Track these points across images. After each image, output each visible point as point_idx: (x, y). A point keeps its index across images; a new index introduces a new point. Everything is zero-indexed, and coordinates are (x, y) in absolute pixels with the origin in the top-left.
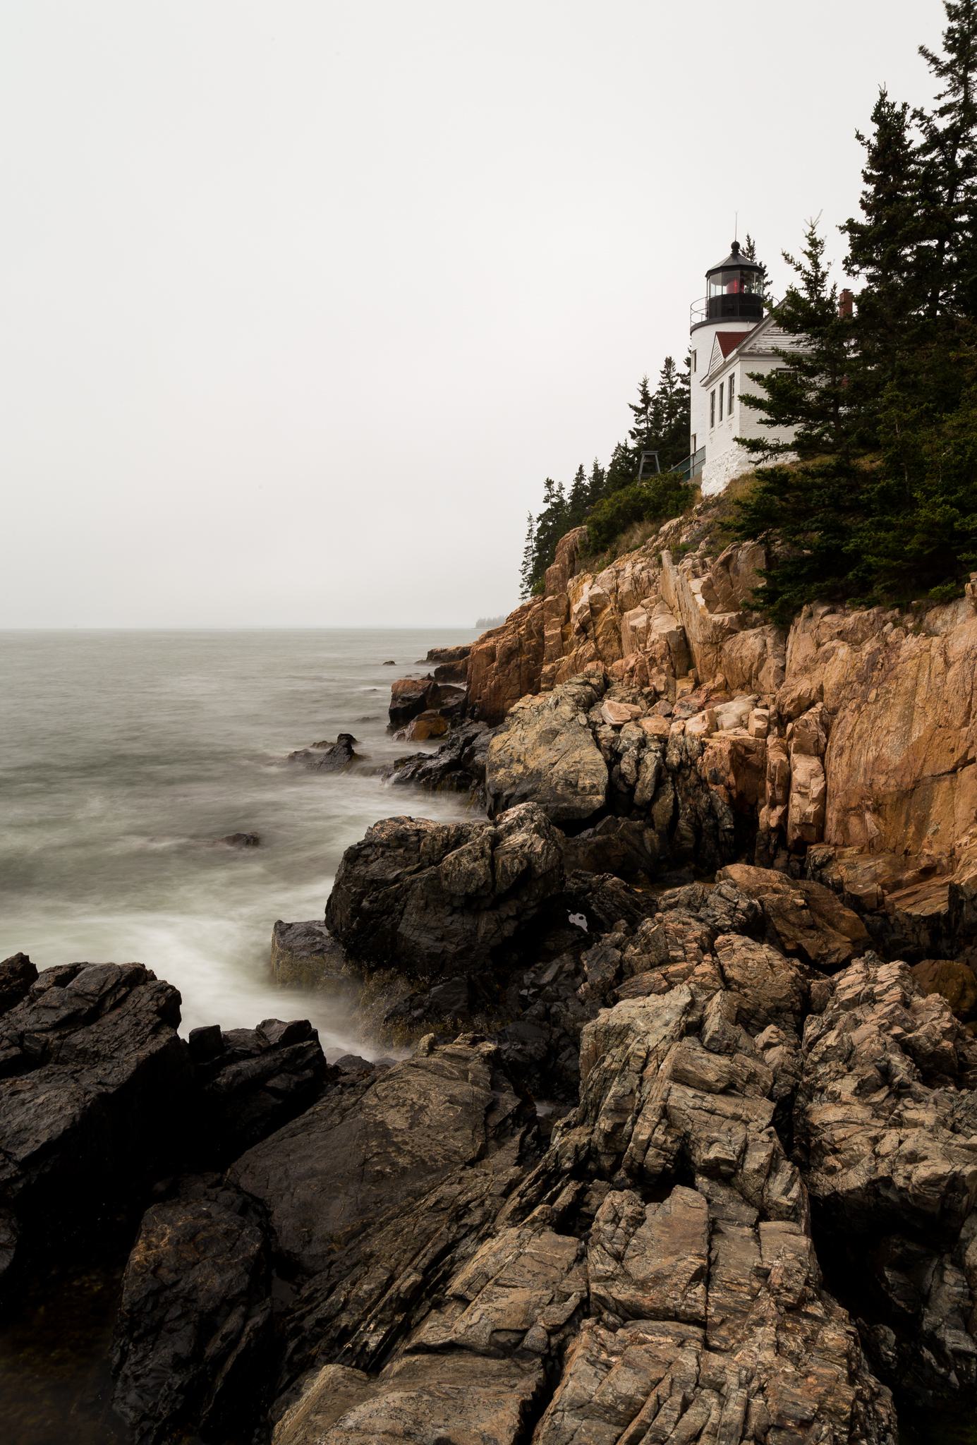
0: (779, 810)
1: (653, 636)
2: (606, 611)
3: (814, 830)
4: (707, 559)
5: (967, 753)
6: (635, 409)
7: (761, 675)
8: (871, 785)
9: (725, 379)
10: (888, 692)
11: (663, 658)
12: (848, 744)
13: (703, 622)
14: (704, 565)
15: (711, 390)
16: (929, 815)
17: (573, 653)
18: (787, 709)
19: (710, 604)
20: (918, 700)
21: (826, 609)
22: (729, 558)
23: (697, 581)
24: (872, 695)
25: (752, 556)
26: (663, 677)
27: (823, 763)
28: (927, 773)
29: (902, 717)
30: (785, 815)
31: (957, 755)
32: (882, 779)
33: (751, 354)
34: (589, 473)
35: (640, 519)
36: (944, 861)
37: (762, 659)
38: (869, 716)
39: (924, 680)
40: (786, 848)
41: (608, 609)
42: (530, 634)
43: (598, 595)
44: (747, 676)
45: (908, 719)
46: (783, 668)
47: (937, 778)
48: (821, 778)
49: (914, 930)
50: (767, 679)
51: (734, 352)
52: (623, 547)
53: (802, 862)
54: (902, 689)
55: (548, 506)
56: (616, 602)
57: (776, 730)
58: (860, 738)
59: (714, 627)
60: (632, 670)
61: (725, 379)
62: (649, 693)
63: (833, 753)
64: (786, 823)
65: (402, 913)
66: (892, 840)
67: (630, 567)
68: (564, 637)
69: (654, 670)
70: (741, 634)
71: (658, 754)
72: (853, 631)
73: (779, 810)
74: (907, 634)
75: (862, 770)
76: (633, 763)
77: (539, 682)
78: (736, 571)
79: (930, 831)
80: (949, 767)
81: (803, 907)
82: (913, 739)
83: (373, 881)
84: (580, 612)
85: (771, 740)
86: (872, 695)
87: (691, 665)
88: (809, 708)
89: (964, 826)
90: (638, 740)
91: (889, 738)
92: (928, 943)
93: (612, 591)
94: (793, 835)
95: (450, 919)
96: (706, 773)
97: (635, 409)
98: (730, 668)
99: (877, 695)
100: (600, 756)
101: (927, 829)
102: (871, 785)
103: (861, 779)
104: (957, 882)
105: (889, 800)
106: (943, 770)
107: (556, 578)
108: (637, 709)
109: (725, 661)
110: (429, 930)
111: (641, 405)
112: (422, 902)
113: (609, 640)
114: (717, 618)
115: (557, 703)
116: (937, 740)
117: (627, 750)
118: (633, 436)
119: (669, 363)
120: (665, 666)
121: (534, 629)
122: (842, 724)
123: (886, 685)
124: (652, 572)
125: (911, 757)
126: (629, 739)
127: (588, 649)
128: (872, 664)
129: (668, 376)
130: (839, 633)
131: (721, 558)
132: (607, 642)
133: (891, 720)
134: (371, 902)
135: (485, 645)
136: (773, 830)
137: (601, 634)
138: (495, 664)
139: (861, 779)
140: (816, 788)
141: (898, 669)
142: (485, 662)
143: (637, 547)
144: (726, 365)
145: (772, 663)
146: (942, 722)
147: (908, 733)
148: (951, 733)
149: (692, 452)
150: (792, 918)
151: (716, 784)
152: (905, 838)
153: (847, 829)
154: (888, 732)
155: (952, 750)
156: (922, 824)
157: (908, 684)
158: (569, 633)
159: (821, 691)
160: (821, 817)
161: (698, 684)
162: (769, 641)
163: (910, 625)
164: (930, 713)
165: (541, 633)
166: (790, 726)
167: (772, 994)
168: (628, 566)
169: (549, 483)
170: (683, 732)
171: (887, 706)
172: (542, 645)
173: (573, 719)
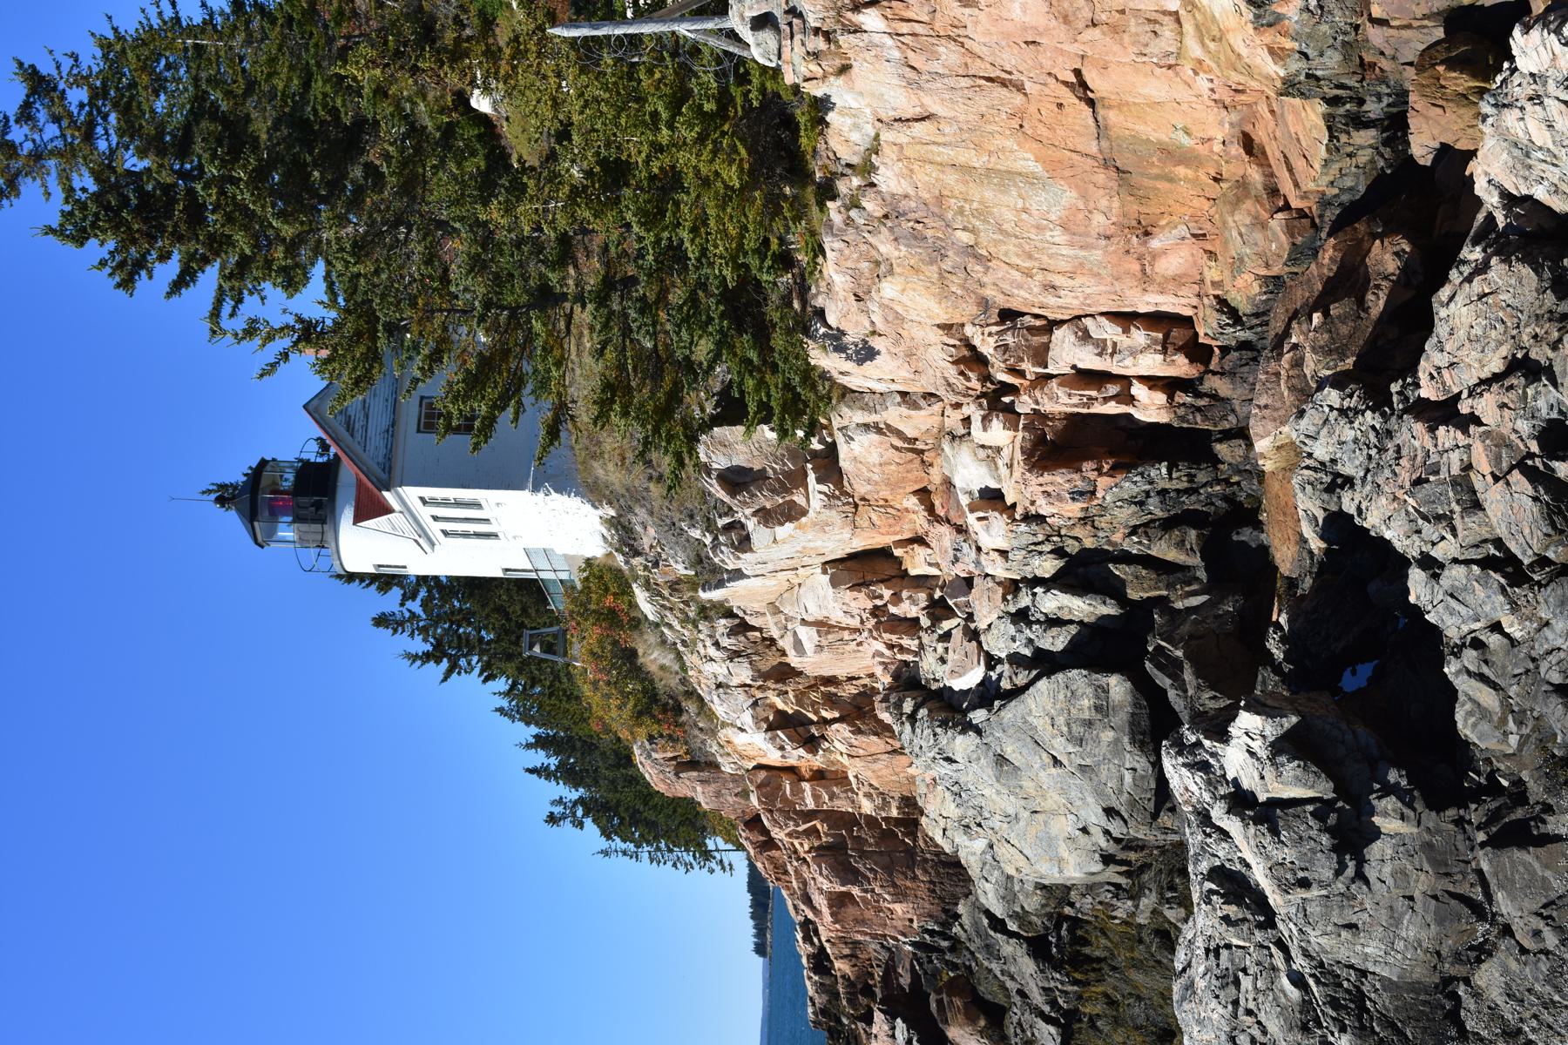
0: (1138, 390)
1: (837, 616)
4: (721, 522)
5: (1066, 83)
7: (910, 433)
8: (1108, 238)
9: (425, 513)
10: (961, 211)
12: (1039, 277)
13: (823, 527)
14: (728, 528)
15: (441, 536)
16: (1160, 142)
17: (845, 760)
18: (975, 384)
19: (792, 513)
20: (978, 161)
23: (754, 538)
27: (1062, 322)
28: (1093, 148)
29: (1003, 188)
31: (1068, 97)
32: (1099, 219)
34: (539, 758)
35: (633, 654)
36: (1234, 117)
38: (996, 243)
39: (947, 154)
40: (1201, 379)
42: (813, 832)
44: (910, 455)
45: (1006, 178)
46: (904, 394)
47: (1101, 130)
48: (1088, 322)
49: (1350, 155)
50: (917, 423)
52: (674, 682)
53: (1225, 350)
55: (588, 822)
57: (1006, 400)
58: (1030, 257)
61: (425, 513)
62: (930, 615)
63: (1051, 300)
65: (1363, 973)
66: (1196, 203)
67: (712, 667)
71: (1038, 590)
72: (855, 275)
73: (1138, 390)
74: (873, 185)
75: (1082, 253)
76: (1055, 631)
79: (1186, 141)
80: (1088, 111)
81: (1326, 314)
82: (1038, 169)
86: (965, 238)
87: (884, 553)
88: (973, 348)
89: (1182, 86)
90: (1014, 622)
92: (1372, 132)
94: (1181, 367)
95: (1376, 885)
96: (1074, 509)
99: (964, 229)
100: (1043, 684)
101: (1180, 147)
102: (1108, 238)
103: (1097, 254)
104: (1279, 84)
106: (1091, 121)
107: (718, 794)
108: (957, 635)
109: (885, 493)
110: (1396, 921)
111: (445, 664)
112: (1344, 934)
114: (816, 502)
115: (949, 760)
116: (1042, 131)
117: (1030, 641)
119: (382, 621)
120: (887, 594)
122: (1006, 286)
123: (950, 216)
124: (721, 630)
125: (1068, 173)
129: (401, 623)
130: (859, 299)
131: (721, 494)
133: (1005, 205)
135: (825, 911)
136: (1171, 397)
137: (816, 713)
138: (856, 891)
140: (1109, 331)
141: (925, 195)
143: (679, 657)
145: (894, 415)
146: (1015, 124)
147: (1029, 179)
148: (1032, 109)
149: (533, 576)
150: (1344, 330)
151: (1093, 493)
152: (1195, 181)
154: (1025, 210)
155: (1060, 106)
156: (1172, 154)
157: (951, 178)
159: (946, 328)
160: (1155, 319)
162: (860, 417)
163: (856, 181)
164: (999, 141)
165: (809, 815)
167: (1530, 296)
168: (709, 668)
169: (552, 819)
170: (1003, 553)
171: (983, 213)
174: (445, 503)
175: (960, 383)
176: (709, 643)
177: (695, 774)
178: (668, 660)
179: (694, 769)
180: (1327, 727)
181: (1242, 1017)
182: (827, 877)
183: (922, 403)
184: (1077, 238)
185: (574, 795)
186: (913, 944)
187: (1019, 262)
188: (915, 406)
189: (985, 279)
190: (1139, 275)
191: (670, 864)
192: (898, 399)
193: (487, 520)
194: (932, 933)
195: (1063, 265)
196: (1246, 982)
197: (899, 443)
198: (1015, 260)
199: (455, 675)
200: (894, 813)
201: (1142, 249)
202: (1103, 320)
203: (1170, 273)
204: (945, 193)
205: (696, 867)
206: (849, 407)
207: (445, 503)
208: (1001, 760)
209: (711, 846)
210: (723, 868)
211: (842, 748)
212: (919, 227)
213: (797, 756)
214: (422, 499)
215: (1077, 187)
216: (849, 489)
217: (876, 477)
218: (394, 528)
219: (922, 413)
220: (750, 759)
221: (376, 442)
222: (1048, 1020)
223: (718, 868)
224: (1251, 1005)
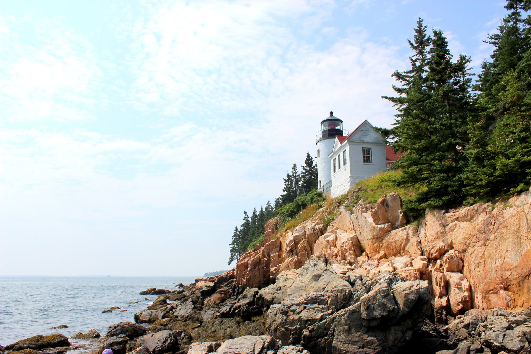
3: (469, 304)
6: (285, 180)
7: (406, 249)
10: (502, 233)
11: (350, 249)
17: (286, 261)
19: (376, 221)
21: (443, 211)
24: (492, 237)
26: (352, 256)
30: (448, 301)
32: (509, 273)
33: (353, 142)
37: (407, 240)
38: (492, 246)
42: (264, 256)
43: (297, 236)
44: (398, 249)
46: (420, 242)
54: (511, 231)
58: (489, 257)
60: (336, 255)
64: (450, 304)
65: (333, 335)
69: (347, 254)
70: (394, 231)
72: (465, 216)
73: (445, 299)
75: (494, 271)
77: (269, 276)
78: (387, 205)
83: (307, 321)
84: (289, 243)
85: (430, 268)
91: (508, 253)
97: (285, 180)
99: (495, 236)
103: (494, 275)
105: (514, 282)
109: (385, 245)
110: (355, 343)
112: (347, 327)
114: (380, 226)
115: (315, 264)
118: (284, 191)
120: (352, 252)
125: (525, 260)
126: (355, 276)
128: (488, 224)
132: (303, 255)
133: (509, 244)
134: (310, 332)
135: (243, 262)
138: (248, 269)
139: (494, 275)
142: (243, 269)
147: (520, 249)
153: (489, 301)
157: (515, 228)
158: (282, 255)
162: (411, 232)
165: (269, 255)
166: (438, 262)
171: (503, 239)
172: (269, 260)
173: (326, 270)
174: (344, 156)
175: (434, 250)
180: (424, 311)
181: (303, 305)
182: (253, 261)
183: (419, 247)
184: (500, 268)
185: (250, 219)
186: (235, 285)
187: (486, 254)
188: (418, 245)
189: (476, 247)
190: (489, 289)
192: (419, 240)
193: (339, 168)
194: (238, 290)
195: (488, 266)
196: (316, 305)
197: (403, 245)
198: (486, 253)
200: (271, 277)
201: (499, 288)
202: (468, 284)
203: (490, 298)
204: (508, 228)
207: (344, 156)
211: (290, 259)
212: (493, 224)
213: (285, 249)
215: (520, 264)
219: (416, 248)
220: (283, 239)
222: (230, 309)
224: (308, 307)
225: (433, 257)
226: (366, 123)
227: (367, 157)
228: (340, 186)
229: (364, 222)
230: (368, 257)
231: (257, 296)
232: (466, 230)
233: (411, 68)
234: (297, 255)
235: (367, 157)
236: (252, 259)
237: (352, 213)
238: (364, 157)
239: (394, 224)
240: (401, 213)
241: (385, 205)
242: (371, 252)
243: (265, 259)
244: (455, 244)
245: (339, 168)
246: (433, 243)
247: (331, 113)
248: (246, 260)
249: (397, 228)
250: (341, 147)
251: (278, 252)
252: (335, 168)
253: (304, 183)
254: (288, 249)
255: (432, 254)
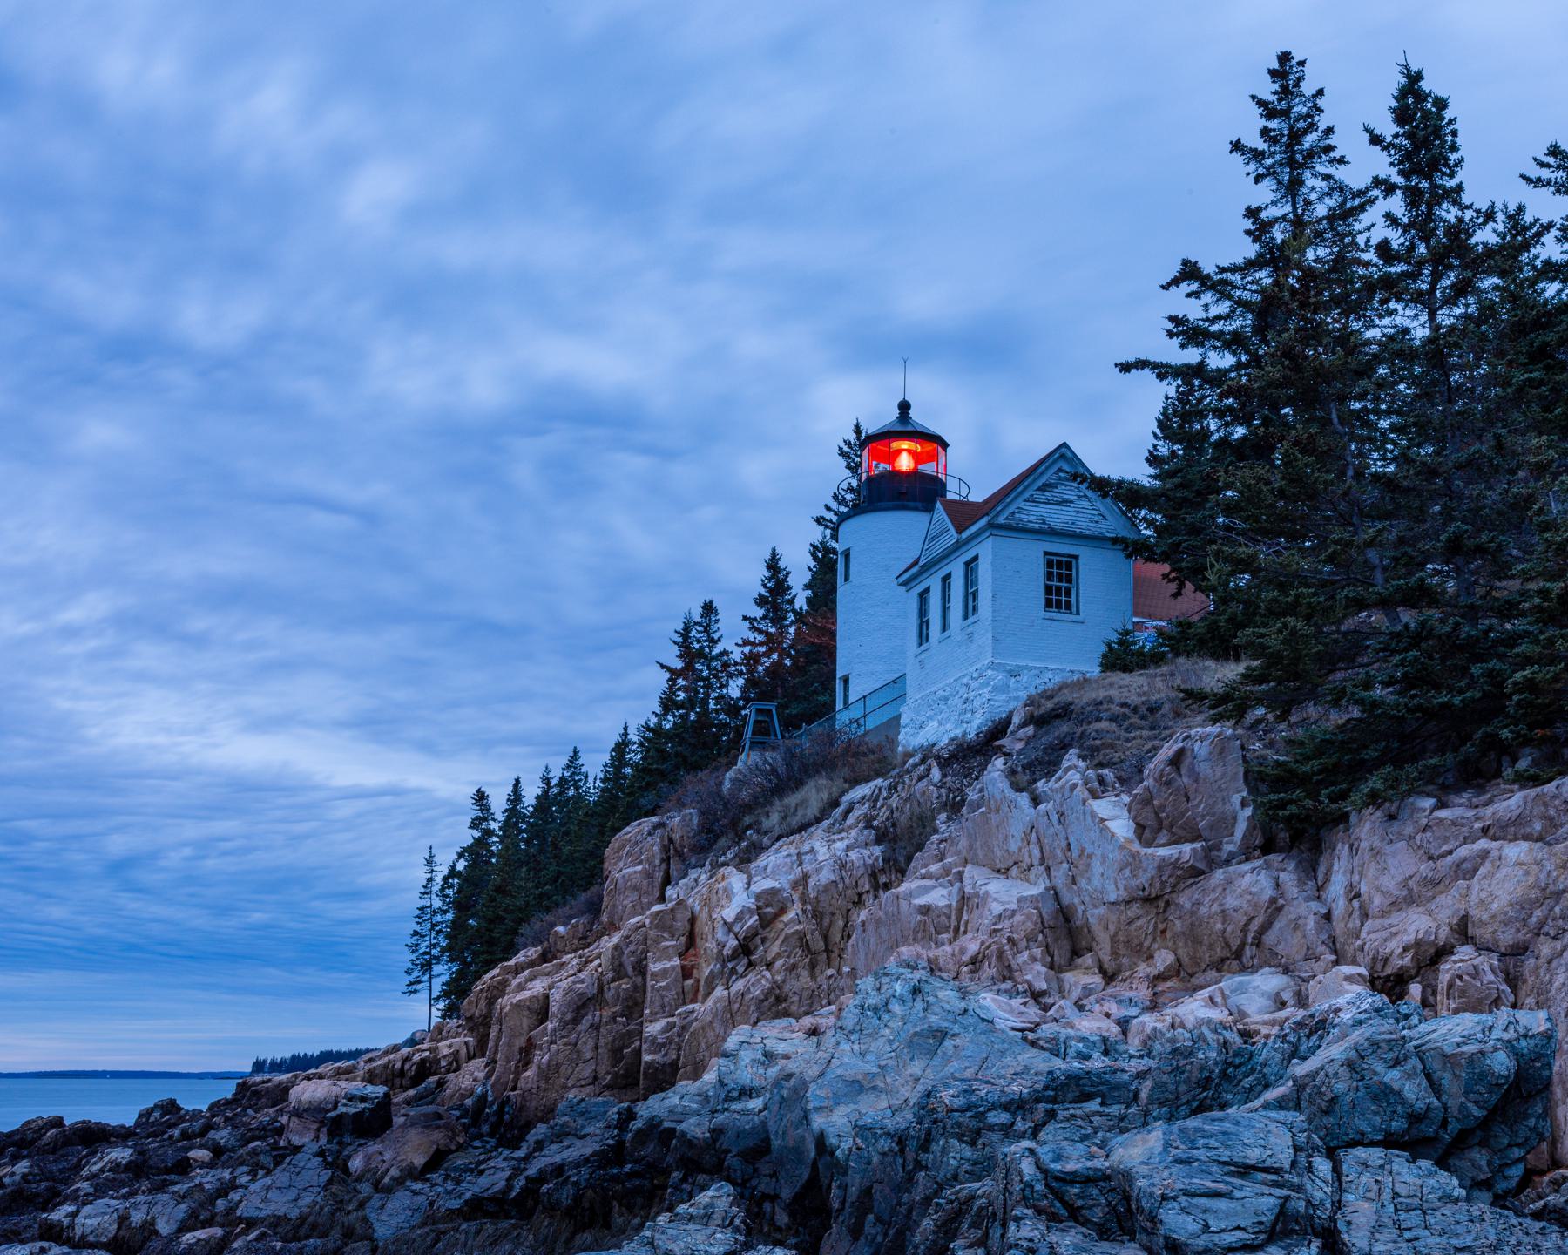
2: (786, 918)
7: (1269, 938)
11: (1030, 938)
13: (1133, 863)
17: (719, 992)
22: (1180, 754)
25: (1221, 748)
26: (1039, 967)
37: (1275, 909)
41: (791, 915)
43: (773, 892)
46: (1328, 917)
51: (983, 521)
56: (804, 900)
59: (1160, 868)
60: (975, 961)
61: (957, 569)
68: (686, 973)
70: (1219, 874)
77: (638, 1052)
84: (739, 918)
93: (795, 885)
98: (1193, 936)
107: (636, 888)
111: (678, 664)
113: (794, 967)
114: (1163, 852)
115: (916, 991)
120: (1038, 952)
121: (628, 961)
124: (866, 852)
127: (755, 983)
130: (1485, 831)
135: (526, 994)
137: (778, 955)
138: (550, 1026)
142: (526, 1023)
144: (958, 546)
159: (1463, 930)
161: (1109, 978)
162: (1288, 878)
165: (640, 968)
166: (1415, 989)
175: (1395, 946)
176: (846, 842)
177: (657, 862)
178: (812, 810)
179: (662, 860)
183: (1324, 936)
188: (1319, 930)
191: (418, 928)
192: (1324, 911)
197: (1254, 926)
199: (668, 675)
200: (647, 1058)
205: (413, 957)
206: (1297, 867)
208: (941, 1035)
209: (437, 969)
210: (412, 984)
214: (976, 558)
216: (1181, 886)
217: (1203, 910)
218: (933, 539)
221: (1032, 513)
223: (412, 978)
225: (1389, 971)
226: (1063, 456)
227: (1059, 590)
228: (946, 699)
229: (1094, 834)
230: (1103, 971)
231: (637, 1124)
232: (1527, 873)
233: (1251, 250)
234: (769, 966)
235: (1059, 589)
236: (564, 984)
237: (1036, 801)
238: (1048, 590)
239: (1218, 847)
240: (1244, 804)
241: (1183, 771)
242: (1115, 954)
243: (625, 985)
244: (1482, 923)
245: (944, 628)
246: (1387, 922)
247: (904, 407)
248: (537, 987)
249: (1227, 862)
250: (958, 546)
251: (680, 955)
252: (923, 623)
253: (752, 683)
254: (732, 943)
255: (1386, 960)
